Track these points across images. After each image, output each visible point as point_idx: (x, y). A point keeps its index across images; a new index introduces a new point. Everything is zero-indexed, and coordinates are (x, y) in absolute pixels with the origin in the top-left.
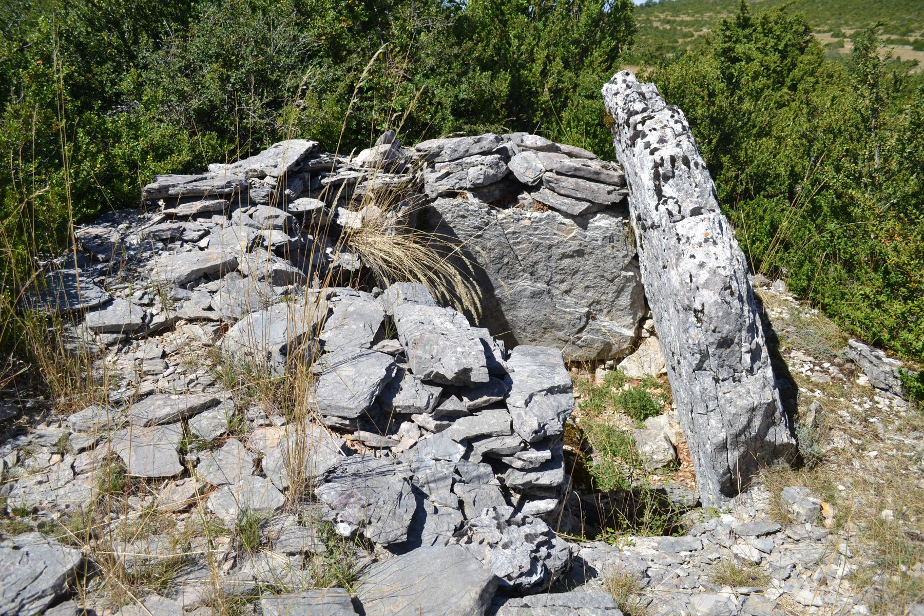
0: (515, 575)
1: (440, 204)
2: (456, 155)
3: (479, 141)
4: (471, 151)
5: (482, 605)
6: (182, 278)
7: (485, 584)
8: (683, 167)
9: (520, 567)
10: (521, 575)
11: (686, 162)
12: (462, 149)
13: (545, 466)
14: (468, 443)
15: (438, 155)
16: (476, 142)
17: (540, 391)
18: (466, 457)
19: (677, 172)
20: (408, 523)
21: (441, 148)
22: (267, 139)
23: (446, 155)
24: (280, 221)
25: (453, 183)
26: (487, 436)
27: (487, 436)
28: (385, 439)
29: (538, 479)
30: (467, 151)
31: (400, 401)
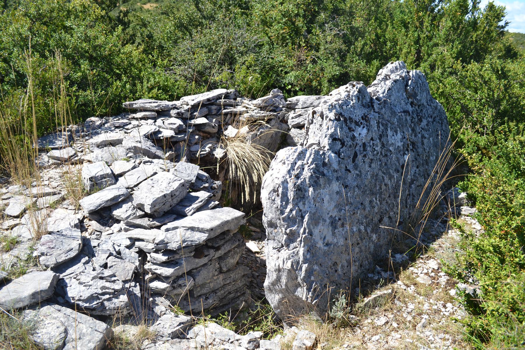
0: (76, 299)
1: (293, 132)
2: (305, 106)
3: (319, 98)
4: (314, 104)
5: (33, 299)
6: (98, 143)
7: (39, 290)
8: (320, 118)
9: (81, 296)
10: (79, 300)
11: (322, 116)
12: (309, 102)
13: (164, 264)
14: (133, 240)
15: (296, 104)
16: (317, 99)
17: (183, 227)
18: (129, 247)
19: (315, 121)
20: (60, 260)
21: (298, 101)
22: (292, 94)
23: (300, 106)
24: (175, 127)
25: (300, 121)
26: (142, 240)
27: (142, 240)
28: (102, 227)
29: (155, 269)
30: (312, 104)
31: (117, 213)
